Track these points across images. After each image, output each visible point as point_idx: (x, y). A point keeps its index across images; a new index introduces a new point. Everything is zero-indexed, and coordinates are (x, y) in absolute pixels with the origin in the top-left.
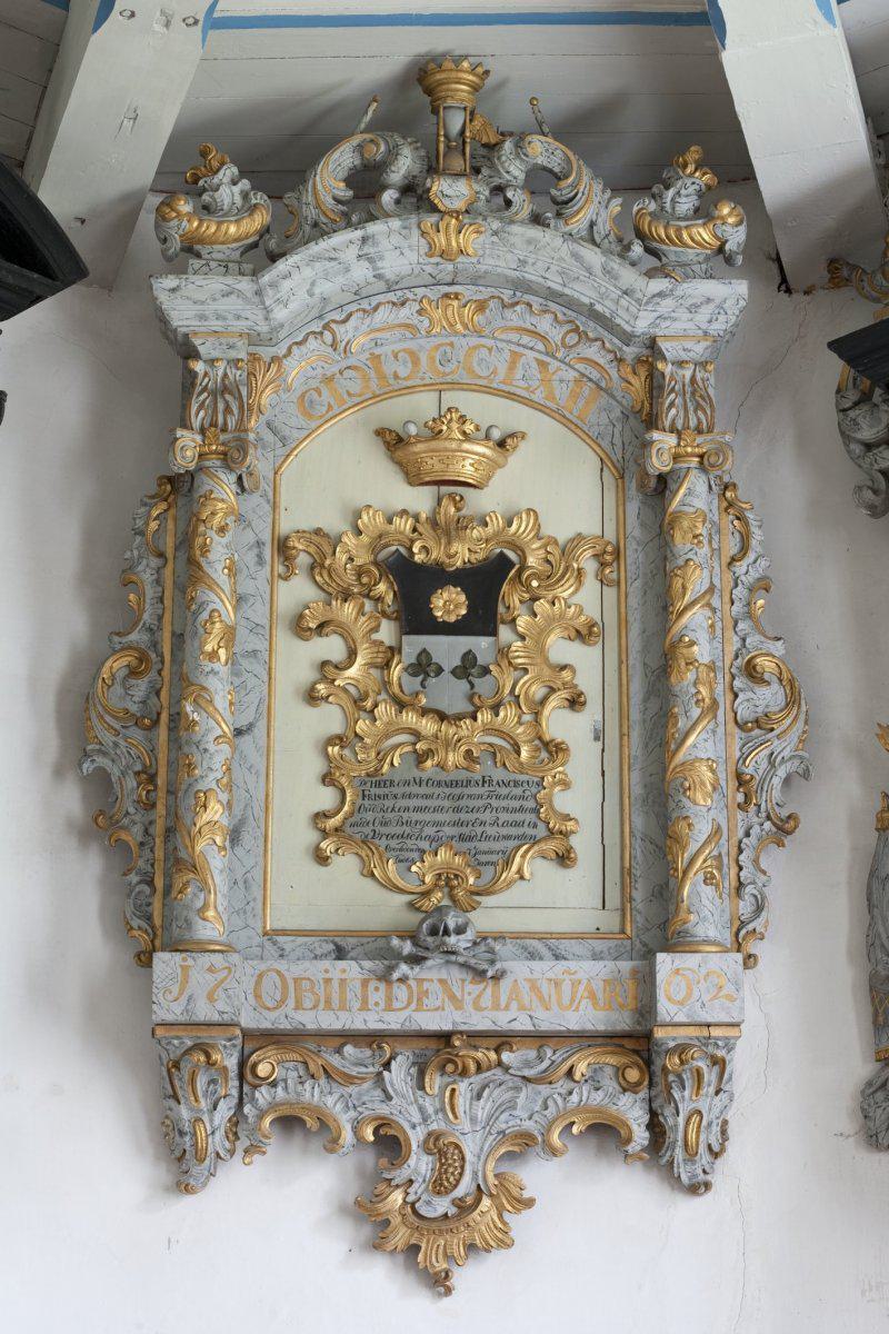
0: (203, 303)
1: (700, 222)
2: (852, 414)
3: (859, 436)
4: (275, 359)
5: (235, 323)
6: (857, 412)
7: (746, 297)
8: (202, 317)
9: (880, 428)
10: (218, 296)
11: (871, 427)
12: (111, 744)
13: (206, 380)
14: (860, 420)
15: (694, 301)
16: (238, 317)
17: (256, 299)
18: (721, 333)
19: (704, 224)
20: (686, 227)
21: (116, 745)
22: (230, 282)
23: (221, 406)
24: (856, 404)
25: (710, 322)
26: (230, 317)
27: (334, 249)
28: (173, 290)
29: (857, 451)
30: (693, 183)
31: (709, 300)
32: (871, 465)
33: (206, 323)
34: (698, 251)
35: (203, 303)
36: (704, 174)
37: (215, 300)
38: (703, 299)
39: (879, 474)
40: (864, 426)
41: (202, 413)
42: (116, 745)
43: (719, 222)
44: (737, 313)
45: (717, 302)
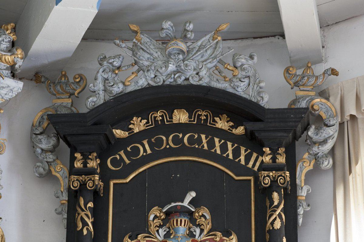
1: (9, 54)
2: (39, 137)
3: (40, 146)
6: (42, 137)
7: (21, 89)
9: (50, 145)
11: (46, 144)
14: (43, 140)
15: (3, 85)
18: (8, 99)
19: (11, 55)
20: (4, 55)
24: (41, 134)
25: (6, 94)
29: (39, 152)
30: (9, 38)
31: (8, 86)
32: (44, 158)
34: (5, 65)
36: (13, 35)
38: (7, 86)
39: (46, 163)
40: (44, 143)
43: (16, 56)
44: (16, 93)
45: (11, 88)
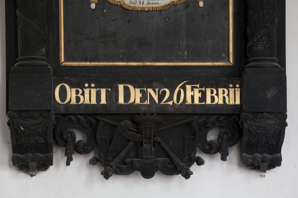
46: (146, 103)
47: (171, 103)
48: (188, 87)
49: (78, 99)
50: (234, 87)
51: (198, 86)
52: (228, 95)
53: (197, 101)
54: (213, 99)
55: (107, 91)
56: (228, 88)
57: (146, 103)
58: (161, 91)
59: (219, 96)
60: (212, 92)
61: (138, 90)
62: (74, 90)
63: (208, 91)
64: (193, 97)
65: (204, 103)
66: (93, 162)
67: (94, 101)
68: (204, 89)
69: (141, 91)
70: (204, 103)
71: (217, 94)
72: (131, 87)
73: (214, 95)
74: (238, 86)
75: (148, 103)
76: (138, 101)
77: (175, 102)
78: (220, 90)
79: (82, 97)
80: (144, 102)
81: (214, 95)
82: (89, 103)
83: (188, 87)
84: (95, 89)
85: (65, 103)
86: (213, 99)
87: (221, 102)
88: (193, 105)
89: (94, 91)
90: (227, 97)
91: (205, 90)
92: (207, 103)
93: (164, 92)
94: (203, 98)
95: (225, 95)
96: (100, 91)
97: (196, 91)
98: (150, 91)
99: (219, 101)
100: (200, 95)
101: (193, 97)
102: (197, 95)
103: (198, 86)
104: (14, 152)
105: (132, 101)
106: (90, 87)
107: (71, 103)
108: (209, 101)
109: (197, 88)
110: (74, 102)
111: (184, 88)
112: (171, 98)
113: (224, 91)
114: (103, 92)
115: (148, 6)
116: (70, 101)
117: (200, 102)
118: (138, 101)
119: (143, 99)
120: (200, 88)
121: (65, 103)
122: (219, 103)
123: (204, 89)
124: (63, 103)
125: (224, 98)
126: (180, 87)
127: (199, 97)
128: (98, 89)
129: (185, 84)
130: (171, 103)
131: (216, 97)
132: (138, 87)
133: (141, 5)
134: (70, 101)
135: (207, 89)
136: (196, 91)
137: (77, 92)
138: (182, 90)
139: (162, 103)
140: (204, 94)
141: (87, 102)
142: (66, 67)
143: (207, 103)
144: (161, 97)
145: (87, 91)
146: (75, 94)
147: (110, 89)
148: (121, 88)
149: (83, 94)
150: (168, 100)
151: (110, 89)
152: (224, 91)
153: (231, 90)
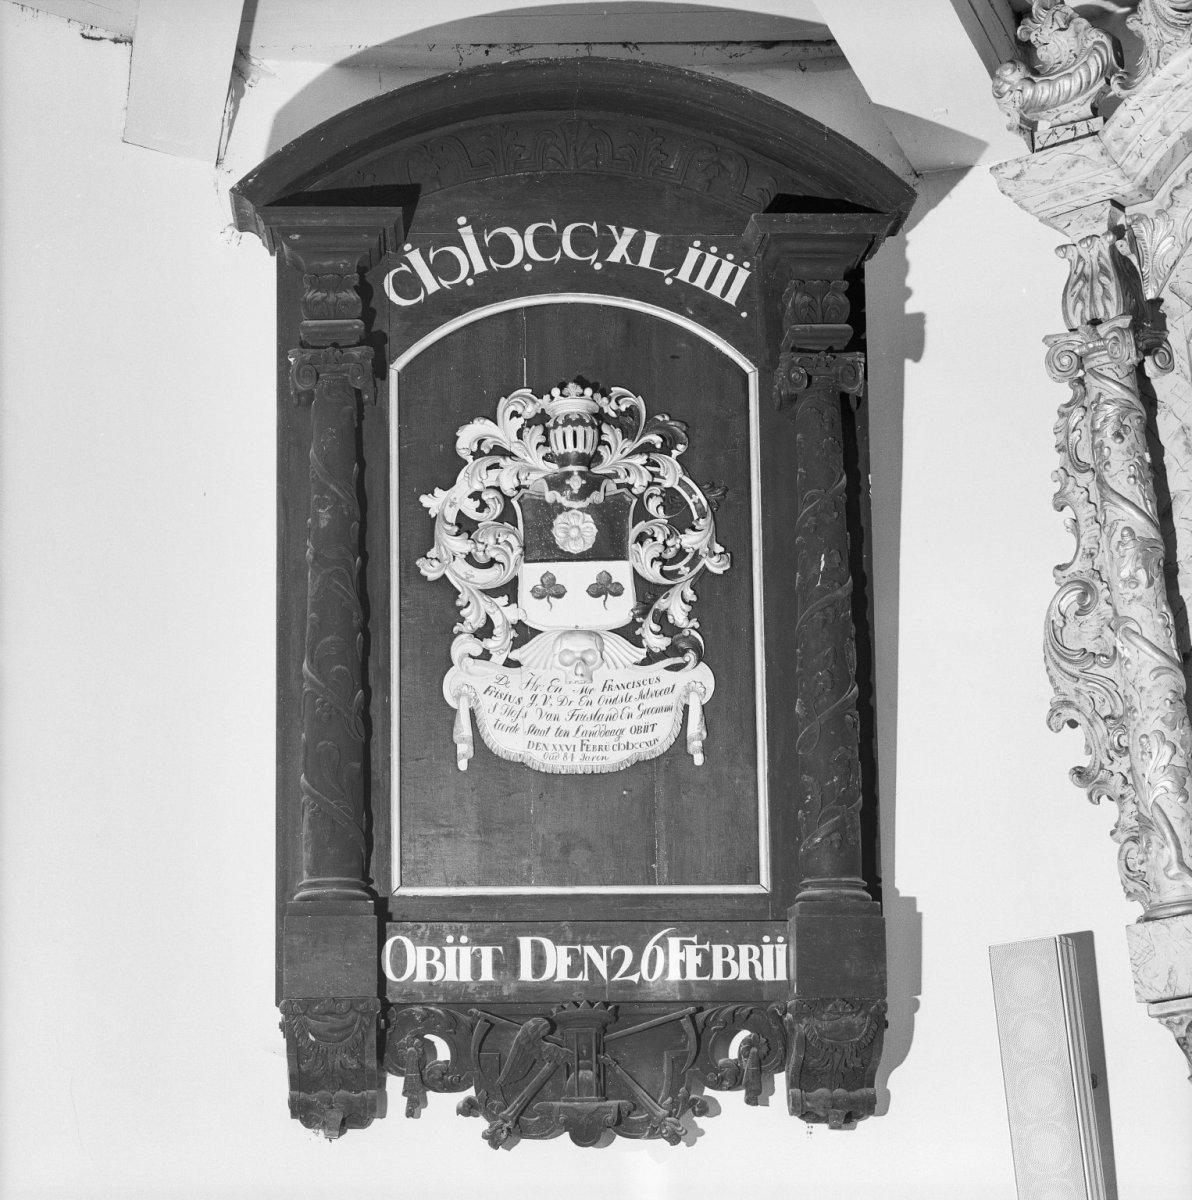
0: (1051, 181)
4: (1160, 212)
5: (1092, 192)
8: (1058, 197)
10: (1064, 169)
12: (1074, 693)
13: (1081, 265)
16: (1094, 186)
17: (1104, 159)
21: (1078, 691)
22: (1071, 151)
23: (1099, 291)
26: (1085, 187)
27: (1175, 76)
28: (1018, 176)
33: (1064, 202)
35: (1051, 181)
37: (1062, 175)
41: (1079, 306)
42: (1078, 691)
46: (579, 978)
47: (635, 978)
48: (674, 943)
49: (431, 971)
50: (773, 942)
51: (694, 939)
52: (760, 959)
53: (692, 975)
54: (727, 969)
55: (496, 953)
56: (759, 943)
57: (579, 978)
58: (613, 952)
59: (741, 962)
60: (725, 954)
61: (563, 949)
62: (422, 950)
63: (717, 950)
64: (683, 966)
65: (707, 978)
66: (468, 1109)
67: (466, 976)
68: (706, 947)
69: (570, 952)
70: (707, 978)
71: (737, 958)
72: (547, 943)
73: (729, 959)
74: (780, 939)
75: (586, 979)
76: (563, 976)
77: (646, 976)
78: (744, 949)
79: (439, 966)
80: (577, 975)
81: (729, 959)
82: (456, 979)
83: (674, 943)
84: (469, 948)
85: (403, 979)
86: (727, 969)
87: (745, 976)
88: (685, 985)
89: (466, 953)
90: (757, 965)
91: (711, 948)
92: (713, 979)
93: (621, 954)
94: (705, 968)
95: (754, 960)
96: (479, 951)
97: (691, 950)
98: (590, 950)
99: (741, 973)
100: (699, 960)
101: (683, 966)
102: (694, 960)
103: (694, 939)
104: (293, 1087)
105: (548, 975)
106: (457, 943)
107: (417, 980)
108: (718, 974)
109: (692, 943)
110: (422, 977)
111: (663, 943)
112: (634, 968)
113: (751, 951)
114: (487, 953)
115: (584, 763)
116: (414, 975)
117: (699, 975)
118: (563, 976)
119: (573, 970)
120: (698, 944)
121: (403, 979)
122: (741, 978)
123: (706, 947)
124: (398, 980)
125: (752, 966)
126: (657, 943)
127: (698, 965)
128: (475, 948)
129: (664, 936)
130: (635, 978)
131: (733, 964)
132: (564, 943)
133: (568, 763)
134: (414, 975)
135: (714, 946)
136: (691, 950)
137: (430, 955)
138: (660, 952)
139: (616, 978)
140: (707, 958)
141: (451, 977)
142: (403, 897)
143: (713, 979)
144: (613, 967)
145: (450, 952)
146: (425, 959)
147: (500, 948)
148: (525, 943)
149: (442, 959)
150: (627, 973)
151: (500, 948)
152: (751, 951)
153: (768, 949)
